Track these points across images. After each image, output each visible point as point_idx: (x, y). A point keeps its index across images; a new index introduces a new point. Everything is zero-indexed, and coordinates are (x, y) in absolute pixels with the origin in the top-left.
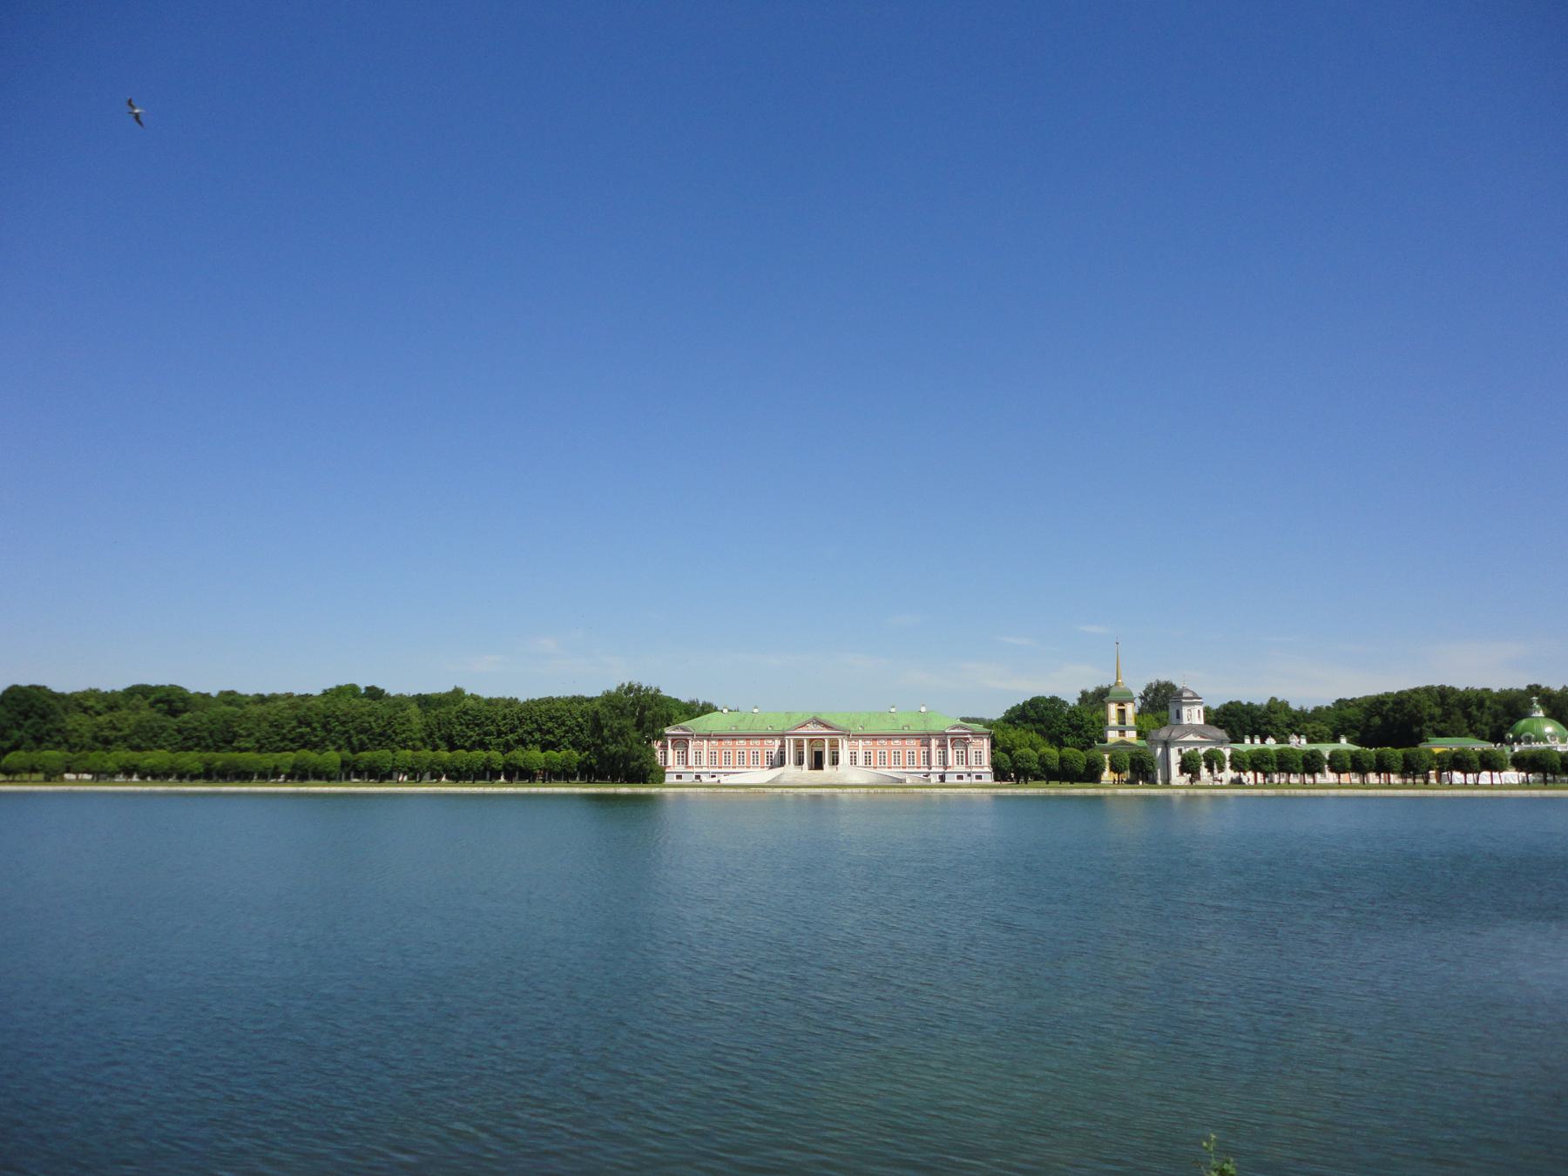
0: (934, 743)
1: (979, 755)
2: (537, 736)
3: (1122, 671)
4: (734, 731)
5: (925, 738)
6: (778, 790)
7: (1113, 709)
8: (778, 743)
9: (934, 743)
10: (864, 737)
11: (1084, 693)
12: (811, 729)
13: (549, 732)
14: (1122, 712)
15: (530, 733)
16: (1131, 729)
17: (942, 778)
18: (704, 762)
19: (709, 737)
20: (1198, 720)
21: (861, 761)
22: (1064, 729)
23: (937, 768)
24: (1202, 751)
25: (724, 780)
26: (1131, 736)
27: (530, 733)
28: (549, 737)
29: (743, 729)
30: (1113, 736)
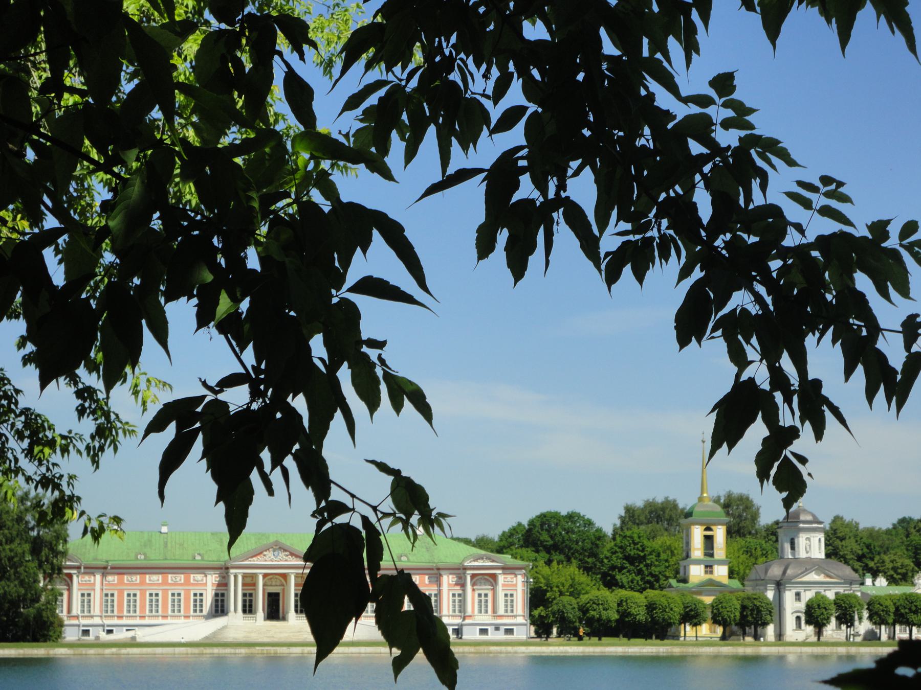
0: (448, 580)
1: (509, 597)
4: (141, 560)
6: (216, 650)
7: (697, 533)
8: (211, 580)
9: (448, 580)
12: (270, 558)
14: (709, 540)
16: (720, 563)
18: (96, 609)
19: (104, 570)
22: (617, 561)
24: (830, 595)
25: (142, 635)
26: (721, 572)
29: (156, 557)
30: (696, 573)
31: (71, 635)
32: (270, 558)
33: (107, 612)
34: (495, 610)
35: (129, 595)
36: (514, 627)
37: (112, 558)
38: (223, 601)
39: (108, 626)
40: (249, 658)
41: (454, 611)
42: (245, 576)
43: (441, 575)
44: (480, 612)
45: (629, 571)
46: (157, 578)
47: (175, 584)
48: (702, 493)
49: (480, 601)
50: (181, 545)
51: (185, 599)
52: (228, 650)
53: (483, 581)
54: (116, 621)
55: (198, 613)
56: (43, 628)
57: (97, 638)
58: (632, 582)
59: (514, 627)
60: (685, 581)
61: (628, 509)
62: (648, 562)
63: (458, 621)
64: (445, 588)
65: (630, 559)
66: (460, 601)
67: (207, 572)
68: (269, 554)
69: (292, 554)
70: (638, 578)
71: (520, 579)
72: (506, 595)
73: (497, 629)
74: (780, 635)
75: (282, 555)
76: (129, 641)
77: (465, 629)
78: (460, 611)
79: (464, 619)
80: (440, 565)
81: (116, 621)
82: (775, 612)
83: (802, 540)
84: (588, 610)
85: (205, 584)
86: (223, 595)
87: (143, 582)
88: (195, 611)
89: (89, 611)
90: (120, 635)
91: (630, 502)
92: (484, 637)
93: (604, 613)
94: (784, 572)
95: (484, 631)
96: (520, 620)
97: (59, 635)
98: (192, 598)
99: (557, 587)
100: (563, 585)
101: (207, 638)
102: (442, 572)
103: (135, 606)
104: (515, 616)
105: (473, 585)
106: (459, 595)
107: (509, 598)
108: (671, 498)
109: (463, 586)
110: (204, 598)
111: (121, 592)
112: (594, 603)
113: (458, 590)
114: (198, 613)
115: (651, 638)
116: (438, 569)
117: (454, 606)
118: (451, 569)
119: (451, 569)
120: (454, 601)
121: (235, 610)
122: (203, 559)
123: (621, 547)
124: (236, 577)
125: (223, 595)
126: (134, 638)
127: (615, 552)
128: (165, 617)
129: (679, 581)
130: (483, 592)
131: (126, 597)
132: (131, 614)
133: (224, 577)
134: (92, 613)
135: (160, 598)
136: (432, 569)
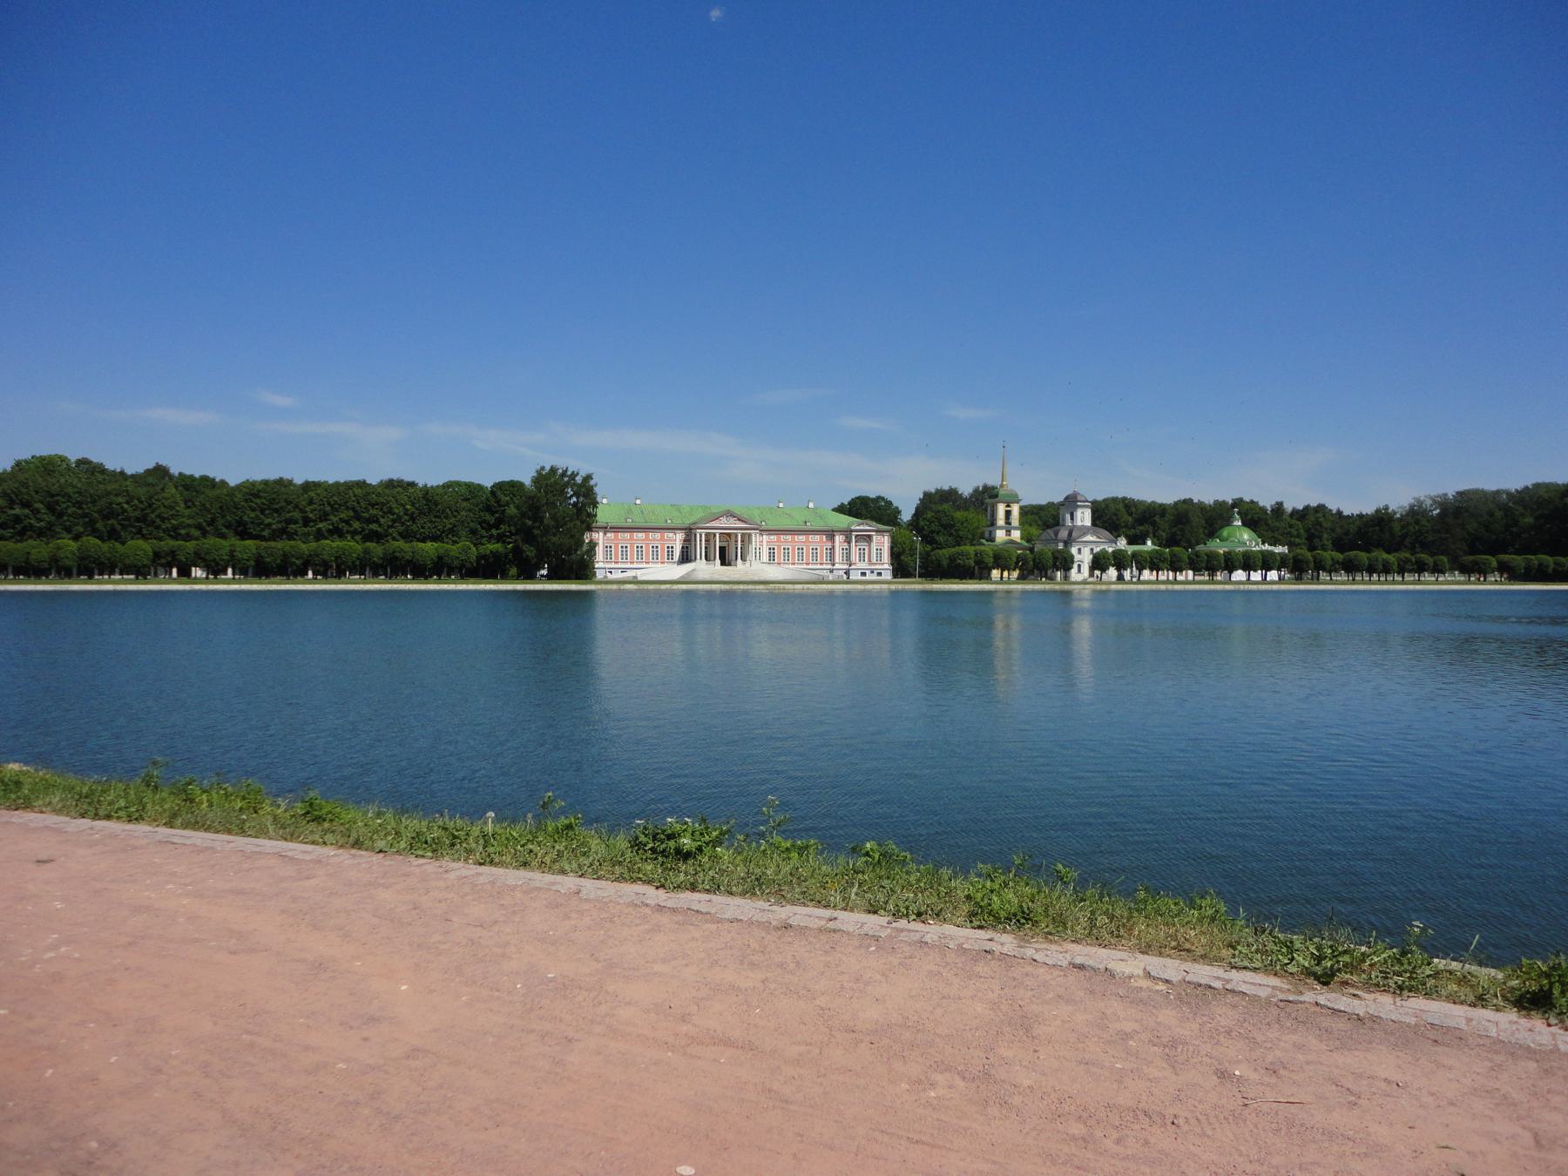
0: (839, 539)
2: (356, 525)
3: (1007, 476)
5: (831, 534)
7: (1001, 509)
8: (680, 536)
9: (839, 539)
10: (770, 532)
12: (724, 522)
13: (369, 521)
14: (1008, 514)
15: (347, 522)
17: (847, 573)
20: (1088, 523)
21: (765, 558)
22: (933, 527)
23: (840, 566)
25: (642, 575)
26: (1016, 535)
27: (347, 522)
28: (374, 526)
29: (640, 522)
30: (1000, 535)
31: (600, 575)
32: (724, 522)
46: (641, 535)
56: (582, 569)
60: (992, 539)
65: (945, 527)
68: (724, 519)
74: (1066, 578)
82: (1064, 562)
83: (1079, 513)
90: (617, 575)
94: (1070, 534)
95: (864, 574)
113: (846, 546)
118: (841, 532)
119: (841, 532)
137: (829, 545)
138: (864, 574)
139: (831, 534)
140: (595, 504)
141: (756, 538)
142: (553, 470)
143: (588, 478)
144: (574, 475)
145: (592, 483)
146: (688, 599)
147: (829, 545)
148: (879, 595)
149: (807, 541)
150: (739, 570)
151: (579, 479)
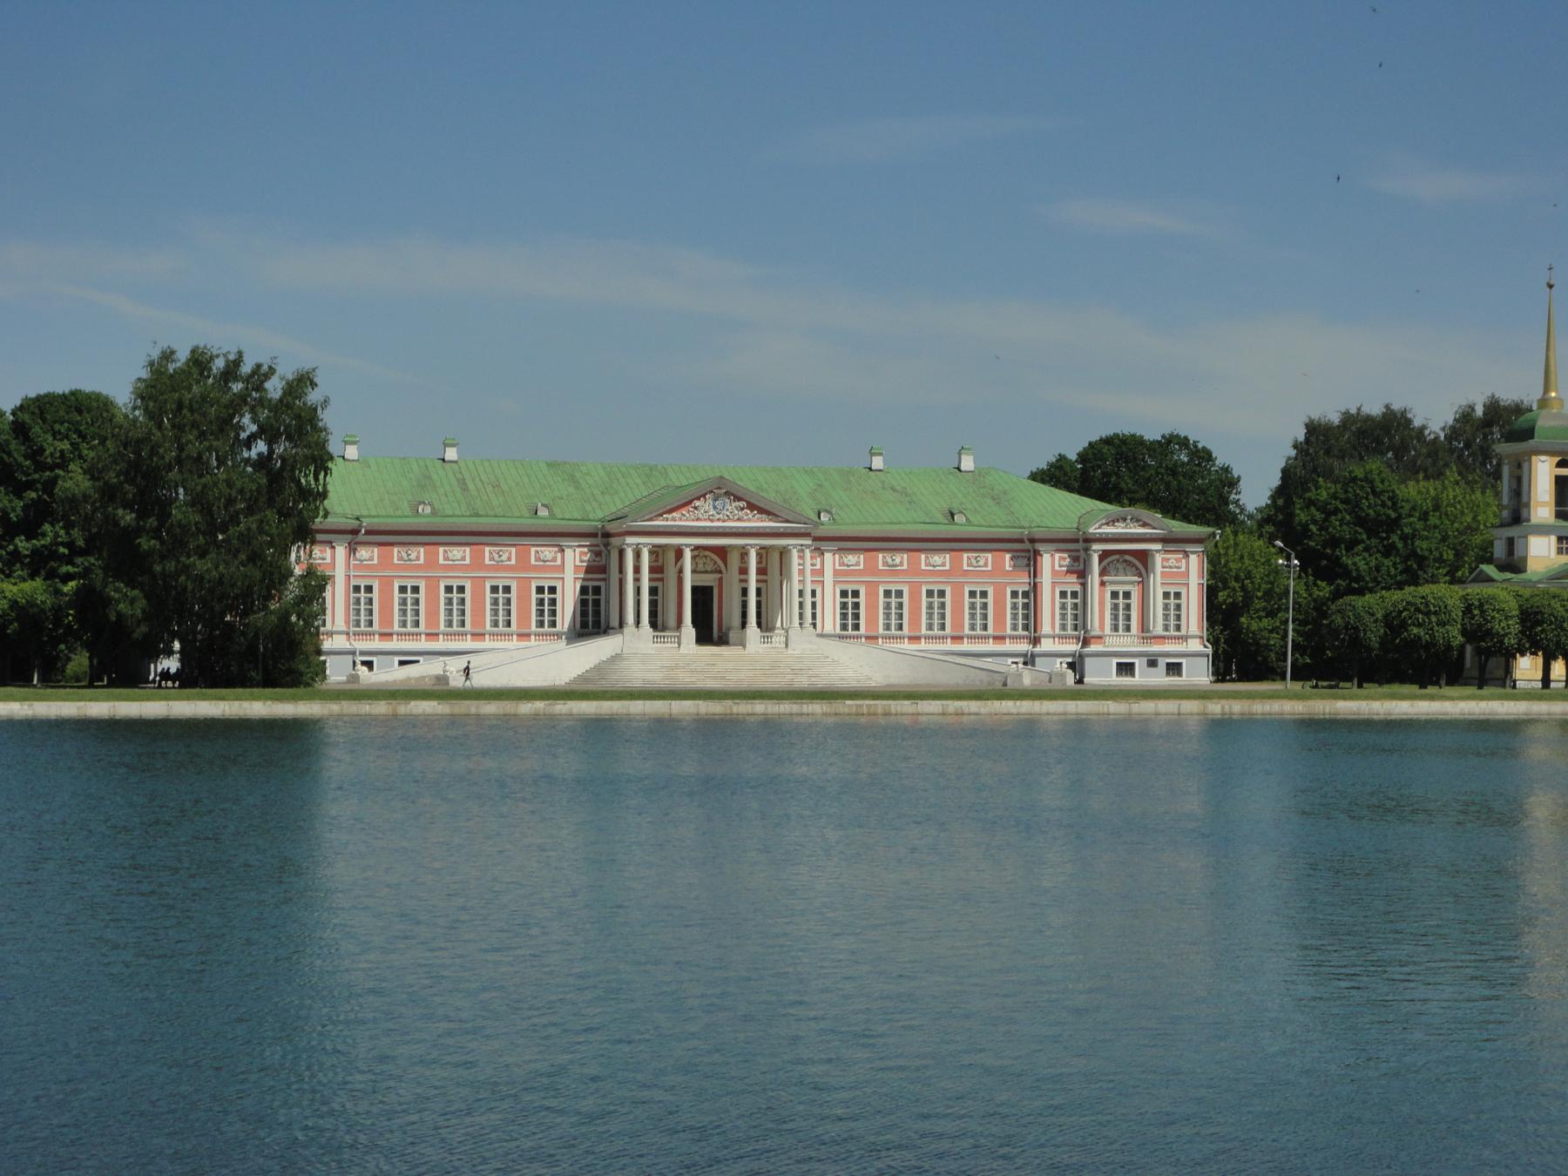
0: (1051, 563)
4: (425, 517)
5: (1027, 550)
8: (574, 558)
9: (1051, 563)
11: (1313, 429)
12: (706, 515)
17: (1076, 665)
21: (830, 620)
22: (1341, 526)
23: (1056, 644)
29: (456, 514)
31: (336, 672)
32: (706, 515)
33: (358, 624)
34: (1144, 627)
35: (403, 589)
36: (1183, 661)
37: (365, 513)
38: (597, 603)
39: (363, 653)
40: (453, 721)
41: (1063, 627)
42: (656, 552)
43: (1037, 553)
44: (1116, 628)
45: (1366, 549)
46: (460, 554)
47: (499, 567)
48: (1546, 390)
49: (1115, 607)
50: (496, 486)
51: (995, 602)
52: (785, 707)
53: (1120, 566)
54: (376, 644)
55: (546, 628)
56: (285, 657)
57: (354, 678)
58: (1378, 569)
59: (1183, 661)
60: (1514, 564)
61: (1313, 429)
62: (1407, 530)
63: (1073, 647)
64: (1046, 579)
66: (1026, 606)
67: (564, 542)
68: (705, 505)
69: (751, 507)
70: (1387, 562)
71: (1193, 559)
72: (1166, 595)
73: (1152, 663)
75: (731, 507)
76: (428, 685)
77: (1089, 663)
78: (1026, 627)
79: (1086, 642)
80: (1038, 533)
81: (376, 644)
84: (1404, 625)
85: (562, 568)
86: (597, 590)
87: (431, 563)
88: (541, 624)
89: (1178, 628)
90: (388, 674)
91: (1316, 415)
92: (1126, 681)
93: (1440, 632)
95: (1126, 669)
96: (1195, 646)
97: (321, 670)
98: (534, 596)
99: (1237, 578)
100: (1249, 575)
101: (582, 678)
102: (1040, 547)
103: (417, 613)
104: (1185, 638)
105: (1102, 573)
106: (1074, 594)
107: (1172, 601)
108: (1396, 407)
109: (1082, 575)
110: (558, 596)
111: (387, 583)
112: (1418, 610)
113: (1072, 583)
114: (546, 628)
115: (1437, 683)
116: (1032, 541)
117: (1063, 617)
120: (1063, 607)
121: (638, 622)
122: (552, 515)
123: (1346, 501)
124: (638, 555)
125: (597, 590)
126: (442, 679)
127: (1336, 511)
128: (478, 636)
129: (1502, 568)
130: (1121, 589)
131: (1009, 600)
132: (409, 629)
133: (598, 554)
134: (1183, 632)
135: (468, 595)
136: (1020, 541)
137: (1022, 582)
138: (1126, 669)
139: (1027, 550)
140: (321, 461)
141: (802, 562)
142: (200, 361)
143: (304, 381)
144: (260, 376)
145: (313, 397)
146: (596, 747)
147: (1022, 582)
148: (1175, 728)
149: (956, 569)
150: (752, 658)
151: (274, 388)
